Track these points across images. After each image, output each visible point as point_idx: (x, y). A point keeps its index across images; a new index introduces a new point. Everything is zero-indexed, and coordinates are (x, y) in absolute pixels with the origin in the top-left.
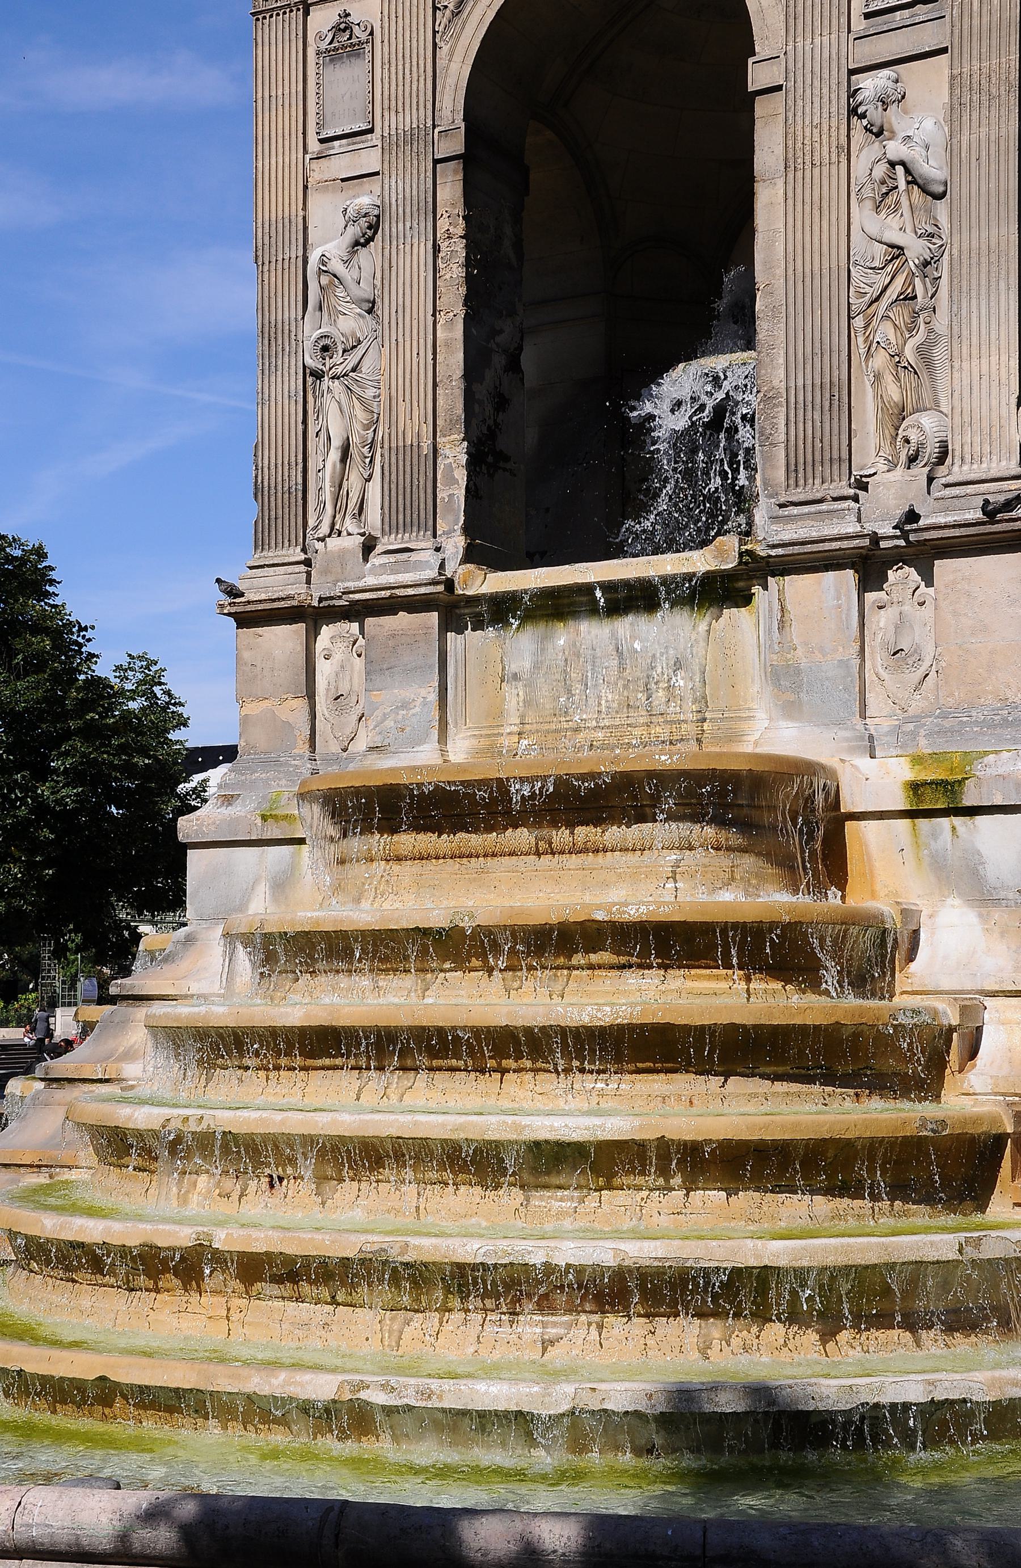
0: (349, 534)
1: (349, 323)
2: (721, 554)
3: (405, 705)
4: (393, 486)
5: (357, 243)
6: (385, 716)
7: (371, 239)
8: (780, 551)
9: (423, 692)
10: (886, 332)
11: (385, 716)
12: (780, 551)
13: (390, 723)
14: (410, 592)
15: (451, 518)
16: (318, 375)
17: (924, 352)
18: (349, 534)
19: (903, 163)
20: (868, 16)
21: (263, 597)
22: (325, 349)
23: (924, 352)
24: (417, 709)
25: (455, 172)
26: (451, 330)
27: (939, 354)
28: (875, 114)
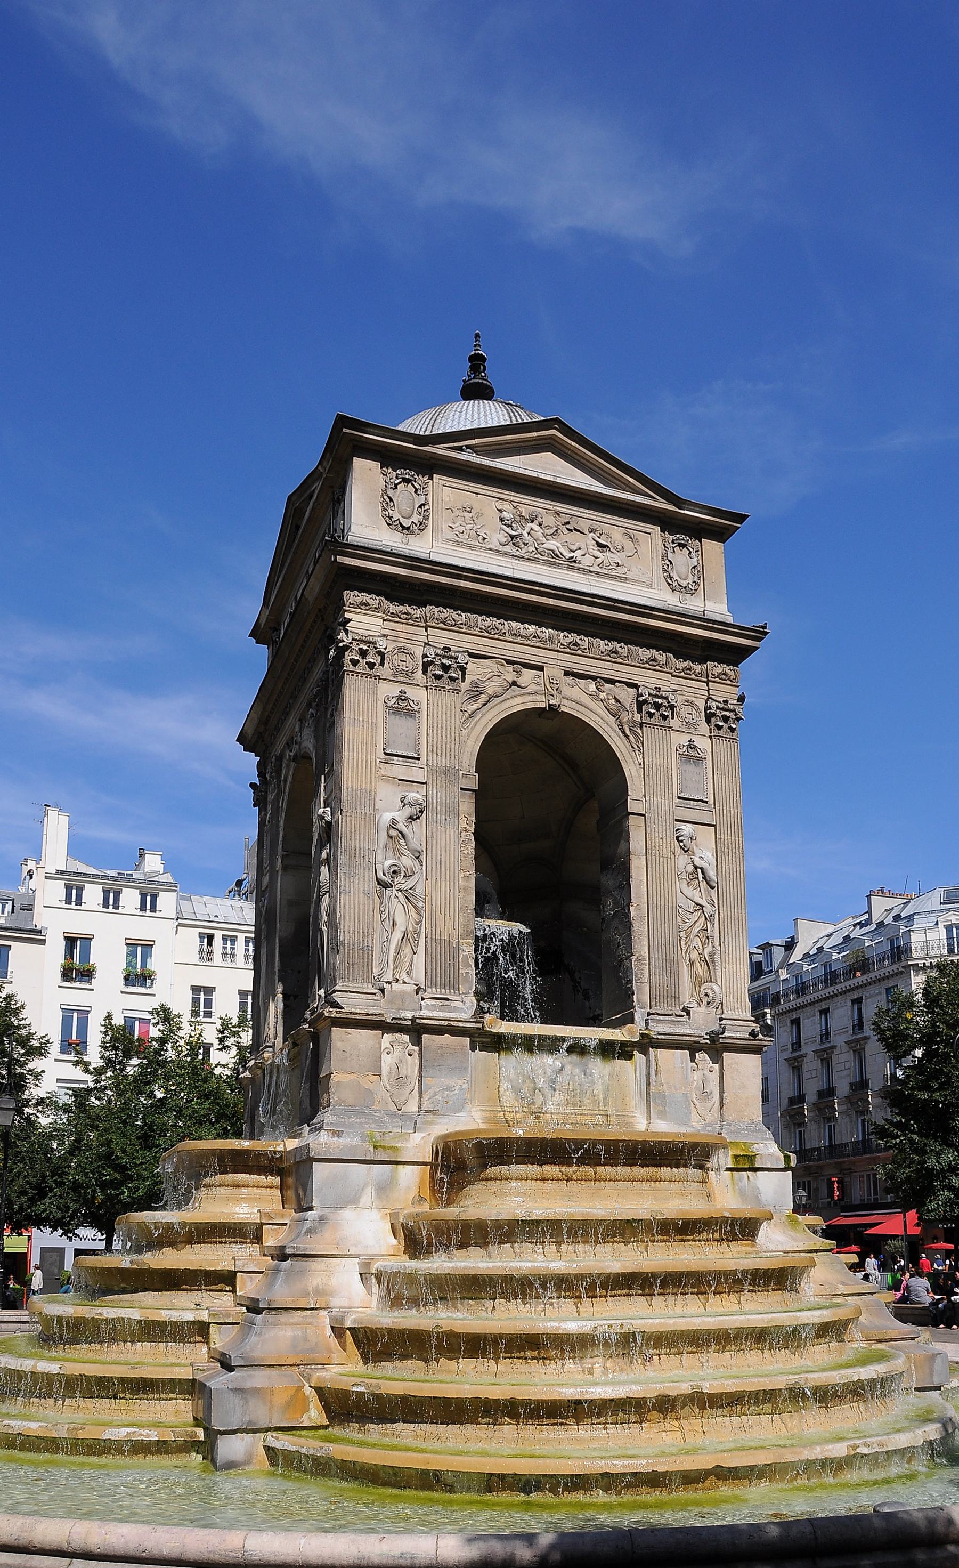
0: (404, 983)
1: (407, 861)
2: (631, 1033)
3: (448, 1088)
4: (434, 961)
5: (410, 818)
6: (435, 1094)
7: (418, 818)
8: (663, 1037)
9: (460, 1082)
10: (697, 942)
11: (435, 1094)
12: (663, 1037)
13: (439, 1097)
14: (460, 1024)
15: (467, 985)
16: (386, 886)
17: (711, 955)
18: (404, 983)
19: (702, 869)
20: (679, 798)
21: (358, 1011)
22: (394, 872)
23: (711, 955)
24: (456, 1092)
25: (470, 797)
26: (467, 881)
27: (717, 957)
28: (687, 842)
